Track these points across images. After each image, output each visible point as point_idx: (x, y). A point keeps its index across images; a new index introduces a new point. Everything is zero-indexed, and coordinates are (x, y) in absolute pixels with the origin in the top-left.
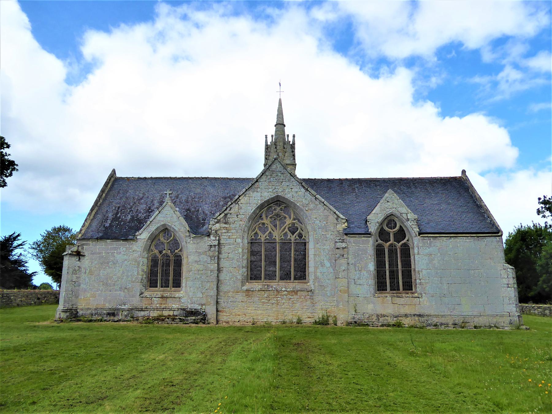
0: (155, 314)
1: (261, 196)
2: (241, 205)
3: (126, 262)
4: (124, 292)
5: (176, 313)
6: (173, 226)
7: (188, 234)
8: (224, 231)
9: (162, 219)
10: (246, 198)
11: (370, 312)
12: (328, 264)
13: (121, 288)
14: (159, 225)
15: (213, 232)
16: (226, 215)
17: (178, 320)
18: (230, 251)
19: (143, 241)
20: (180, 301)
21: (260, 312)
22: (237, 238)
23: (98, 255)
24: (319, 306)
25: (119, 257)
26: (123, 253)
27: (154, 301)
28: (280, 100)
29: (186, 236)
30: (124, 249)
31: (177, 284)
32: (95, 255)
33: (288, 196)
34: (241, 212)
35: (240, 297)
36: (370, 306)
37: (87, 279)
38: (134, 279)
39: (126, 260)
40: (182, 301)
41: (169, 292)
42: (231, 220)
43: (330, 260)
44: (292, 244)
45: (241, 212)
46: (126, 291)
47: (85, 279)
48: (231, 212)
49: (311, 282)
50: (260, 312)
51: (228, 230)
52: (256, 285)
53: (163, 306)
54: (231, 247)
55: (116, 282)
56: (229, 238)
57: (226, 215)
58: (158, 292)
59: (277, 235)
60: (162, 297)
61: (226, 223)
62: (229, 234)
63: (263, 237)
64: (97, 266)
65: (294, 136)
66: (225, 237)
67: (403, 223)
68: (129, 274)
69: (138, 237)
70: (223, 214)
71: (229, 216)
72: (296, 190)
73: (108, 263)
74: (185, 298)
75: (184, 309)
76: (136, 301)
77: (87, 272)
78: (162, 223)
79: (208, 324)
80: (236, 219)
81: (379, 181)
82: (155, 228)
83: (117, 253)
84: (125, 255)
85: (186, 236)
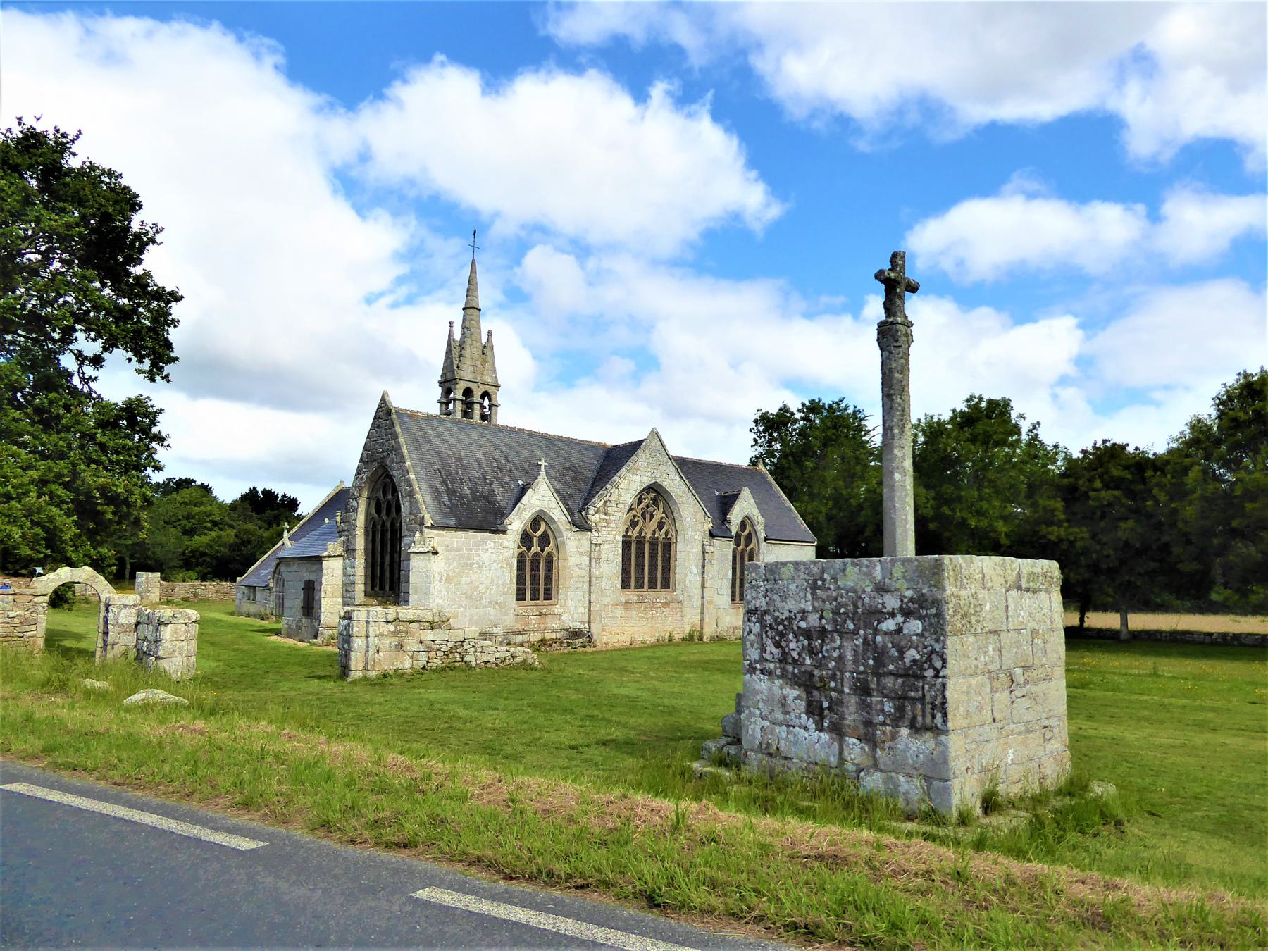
0: (535, 638)
1: (641, 481)
2: (621, 491)
3: (495, 564)
4: (494, 608)
5: (558, 635)
6: (551, 514)
7: (569, 527)
8: (604, 524)
9: (538, 502)
10: (626, 482)
11: (727, 624)
12: (695, 571)
13: (490, 603)
14: (534, 511)
15: (594, 524)
16: (606, 502)
17: (565, 645)
18: (609, 552)
19: (515, 533)
20: (560, 619)
21: (636, 629)
22: (616, 535)
23: (457, 553)
24: (686, 620)
25: (486, 557)
26: (490, 550)
27: (531, 619)
28: (473, 263)
29: (567, 529)
30: (492, 544)
31: (548, 596)
32: (453, 553)
33: (665, 484)
34: (622, 499)
35: (619, 611)
36: (728, 618)
37: (444, 590)
38: (506, 590)
39: (495, 561)
40: (563, 618)
41: (544, 606)
42: (610, 509)
43: (697, 566)
44: (660, 546)
45: (622, 499)
46: (497, 607)
47: (440, 591)
48: (611, 499)
49: (679, 591)
50: (636, 629)
51: (607, 522)
52: (632, 596)
53: (542, 627)
54: (611, 545)
55: (483, 594)
56: (609, 534)
57: (606, 502)
58: (529, 607)
59: (648, 534)
60: (541, 614)
61: (605, 514)
62: (609, 529)
63: (634, 533)
64: (457, 570)
65: (490, 333)
66: (605, 533)
67: (752, 525)
68: (500, 582)
69: (509, 527)
70: (603, 501)
71: (608, 504)
72: (673, 477)
73: (471, 565)
74: (566, 615)
75: (567, 630)
76: (510, 622)
77: (444, 578)
78: (538, 509)
79: (594, 647)
80: (616, 509)
81: (701, 464)
82: (529, 516)
83: (483, 551)
84: (492, 553)
85: (567, 529)
